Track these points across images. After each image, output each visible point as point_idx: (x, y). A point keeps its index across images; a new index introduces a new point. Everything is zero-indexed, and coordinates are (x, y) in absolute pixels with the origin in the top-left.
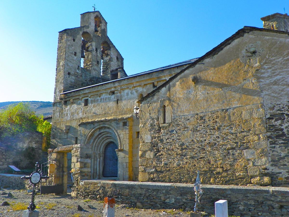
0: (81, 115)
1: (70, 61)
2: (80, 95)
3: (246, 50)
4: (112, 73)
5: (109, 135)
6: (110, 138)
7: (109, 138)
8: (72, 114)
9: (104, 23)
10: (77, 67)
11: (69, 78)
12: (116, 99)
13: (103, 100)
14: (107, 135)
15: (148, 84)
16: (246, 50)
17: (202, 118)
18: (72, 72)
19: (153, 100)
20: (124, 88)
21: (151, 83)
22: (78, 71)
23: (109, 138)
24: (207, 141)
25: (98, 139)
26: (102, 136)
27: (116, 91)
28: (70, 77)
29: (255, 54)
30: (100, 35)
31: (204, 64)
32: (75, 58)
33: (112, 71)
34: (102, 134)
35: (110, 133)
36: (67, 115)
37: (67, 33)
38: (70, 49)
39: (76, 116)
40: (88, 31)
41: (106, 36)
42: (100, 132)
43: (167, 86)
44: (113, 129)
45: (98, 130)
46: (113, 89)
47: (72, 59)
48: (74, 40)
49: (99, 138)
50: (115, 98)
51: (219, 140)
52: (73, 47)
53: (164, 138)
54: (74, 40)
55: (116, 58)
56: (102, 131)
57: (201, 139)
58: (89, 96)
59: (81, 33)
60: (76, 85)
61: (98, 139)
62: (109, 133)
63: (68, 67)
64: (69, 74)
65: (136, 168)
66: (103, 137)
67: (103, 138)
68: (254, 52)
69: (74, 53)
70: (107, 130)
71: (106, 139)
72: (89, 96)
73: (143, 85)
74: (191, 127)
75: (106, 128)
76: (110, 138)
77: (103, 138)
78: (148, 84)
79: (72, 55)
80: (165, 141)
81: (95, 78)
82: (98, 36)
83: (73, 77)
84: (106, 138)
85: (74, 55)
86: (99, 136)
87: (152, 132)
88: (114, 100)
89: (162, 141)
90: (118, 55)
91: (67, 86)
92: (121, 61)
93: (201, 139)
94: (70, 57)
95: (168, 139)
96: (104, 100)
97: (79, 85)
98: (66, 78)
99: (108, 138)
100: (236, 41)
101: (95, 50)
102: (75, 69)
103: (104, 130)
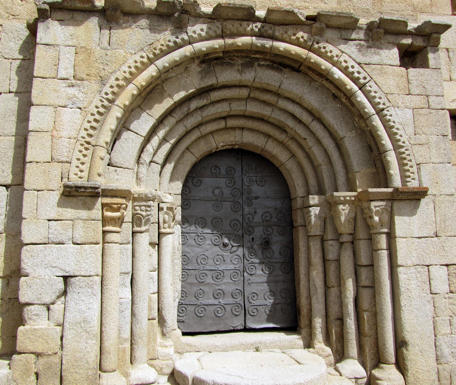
5: (253, 108)
6: (242, 129)
7: (234, 129)
14: (237, 108)
23: (234, 129)
25: (177, 122)
34: (215, 95)
42: (210, 81)
45: (195, 68)
49: (188, 115)
56: (227, 75)
66: (212, 111)
75: (259, 65)
76: (242, 129)
84: (222, 124)
86: (194, 105)
99: (231, 123)
103: (241, 72)
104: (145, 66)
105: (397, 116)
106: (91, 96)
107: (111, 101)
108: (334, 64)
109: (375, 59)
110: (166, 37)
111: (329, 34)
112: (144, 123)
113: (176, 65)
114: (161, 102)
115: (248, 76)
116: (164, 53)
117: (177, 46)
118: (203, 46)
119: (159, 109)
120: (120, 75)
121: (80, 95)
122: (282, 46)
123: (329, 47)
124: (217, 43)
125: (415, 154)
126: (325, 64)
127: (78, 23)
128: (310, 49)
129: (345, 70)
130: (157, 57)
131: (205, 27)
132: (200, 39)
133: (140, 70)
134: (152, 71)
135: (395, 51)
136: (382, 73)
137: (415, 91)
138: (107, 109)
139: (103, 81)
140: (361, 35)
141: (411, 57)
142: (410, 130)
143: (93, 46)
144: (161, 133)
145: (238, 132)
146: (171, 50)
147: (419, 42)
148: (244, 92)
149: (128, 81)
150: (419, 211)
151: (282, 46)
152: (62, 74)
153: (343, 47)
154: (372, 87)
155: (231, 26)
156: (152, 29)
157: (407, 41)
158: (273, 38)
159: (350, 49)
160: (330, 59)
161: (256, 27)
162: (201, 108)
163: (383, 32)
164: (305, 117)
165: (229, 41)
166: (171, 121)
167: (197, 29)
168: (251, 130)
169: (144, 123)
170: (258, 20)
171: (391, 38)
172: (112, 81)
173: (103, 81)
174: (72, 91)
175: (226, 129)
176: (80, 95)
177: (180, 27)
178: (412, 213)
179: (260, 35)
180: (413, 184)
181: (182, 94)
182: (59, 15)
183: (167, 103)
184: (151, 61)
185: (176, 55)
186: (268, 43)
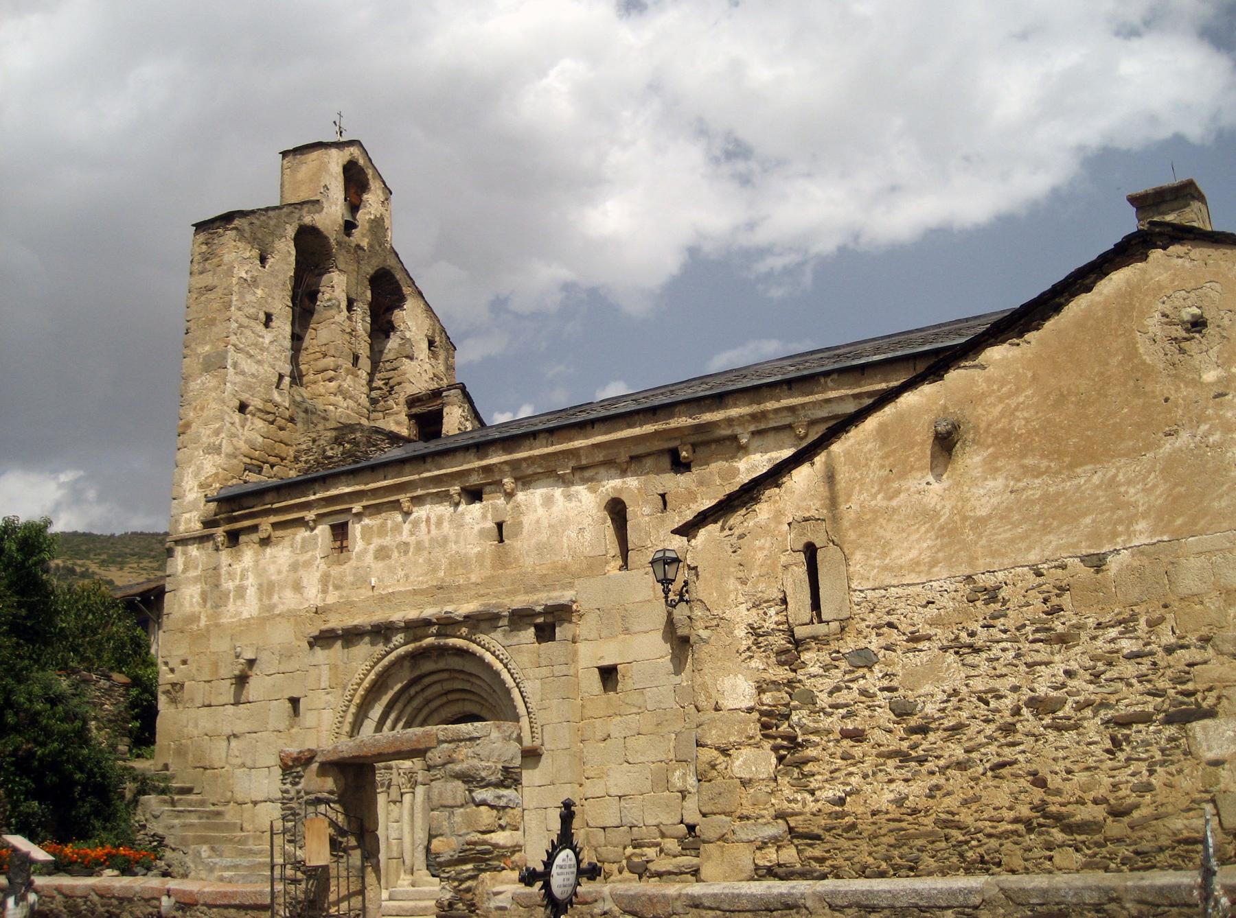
0: (313, 595)
1: (248, 353)
2: (307, 506)
3: (1165, 315)
4: (414, 411)
5: (458, 685)
7: (458, 700)
8: (267, 589)
9: (380, 192)
10: (275, 380)
11: (243, 427)
12: (490, 524)
13: (423, 526)
14: (448, 686)
15: (649, 455)
16: (1165, 315)
17: (992, 594)
18: (256, 402)
19: (751, 524)
20: (530, 471)
21: (661, 452)
22: (276, 397)
24: (1026, 694)
25: (405, 706)
26: (423, 690)
27: (490, 484)
28: (249, 424)
29: (1200, 332)
30: (365, 243)
31: (983, 367)
32: (268, 337)
33: (413, 401)
34: (427, 681)
35: (466, 677)
36: (241, 592)
37: (236, 228)
38: (249, 298)
39: (288, 600)
40: (319, 225)
41: (388, 246)
42: (417, 673)
43: (819, 460)
44: (488, 657)
45: (407, 664)
46: (475, 480)
47: (256, 345)
48: (263, 260)
49: (411, 699)
50: (484, 517)
51: (1073, 683)
52: (259, 292)
53: (821, 688)
54: (263, 260)
55: (425, 345)
56: (428, 666)
57: (997, 684)
58: (354, 511)
59: (291, 231)
60: (272, 459)
61: (405, 706)
62: (462, 676)
63: (239, 379)
64: (242, 408)
65: (604, 828)
66: (428, 692)
67: (428, 702)
68: (1198, 324)
69: (262, 316)
70: (456, 663)
71: (442, 706)
72: (354, 511)
73: (623, 457)
74: (942, 635)
77: (428, 702)
78: (649, 455)
79: (253, 323)
80: (823, 700)
81: (362, 431)
82: (358, 246)
83: (260, 424)
84: (444, 699)
85: (261, 327)
86: (412, 691)
87: (755, 663)
88: (482, 525)
89: (809, 699)
90: (434, 331)
91: (235, 461)
92: (447, 359)
93: (997, 684)
94: (248, 332)
95: (838, 689)
96: (433, 527)
97: (283, 459)
98: (233, 430)
99: (451, 697)
100: (1118, 278)
101: (344, 305)
102: (268, 390)
103: (436, 662)
104: (369, 671)
105: (528, 687)
106: (336, 700)
107: (350, 701)
108: (488, 650)
109: (515, 641)
110: (380, 648)
111: (483, 626)
112: (376, 712)
113: (393, 664)
114: (386, 693)
115: (441, 665)
116: (380, 660)
117: (388, 653)
118: (401, 651)
119: (386, 699)
120: (355, 681)
121: (332, 699)
122: (451, 641)
123: (483, 637)
124: (410, 647)
125: (540, 717)
126: (479, 650)
127: (329, 646)
128: (471, 640)
129: (493, 653)
130: (376, 663)
131: (402, 635)
132: (400, 646)
133: (366, 675)
134: (372, 676)
135: (532, 629)
136: (520, 651)
137: (543, 663)
138: (348, 707)
139: (344, 688)
140: (506, 622)
141: (545, 633)
142: (538, 697)
143: (339, 662)
144: (392, 716)
145: (460, 704)
146: (384, 657)
147: (550, 619)
148: (445, 675)
149: (359, 685)
150: (541, 764)
151: (451, 641)
152: (323, 686)
153: (492, 635)
154: (512, 666)
155: (419, 632)
156: (373, 643)
157: (540, 620)
158: (448, 636)
159: (498, 635)
160: (483, 647)
161: (434, 629)
162: (423, 690)
163: (520, 618)
164: (487, 688)
165: (418, 644)
166: (399, 705)
167: (399, 638)
168: (471, 701)
169: (376, 712)
170: (435, 624)
171: (528, 620)
172: (350, 687)
173: (344, 688)
174: (328, 697)
175: (449, 702)
176: (332, 699)
177: (387, 640)
178: (535, 766)
179: (438, 635)
180: (537, 742)
181: (399, 686)
182: (320, 643)
183: (390, 694)
184: (373, 667)
185: (386, 661)
186: (442, 641)
